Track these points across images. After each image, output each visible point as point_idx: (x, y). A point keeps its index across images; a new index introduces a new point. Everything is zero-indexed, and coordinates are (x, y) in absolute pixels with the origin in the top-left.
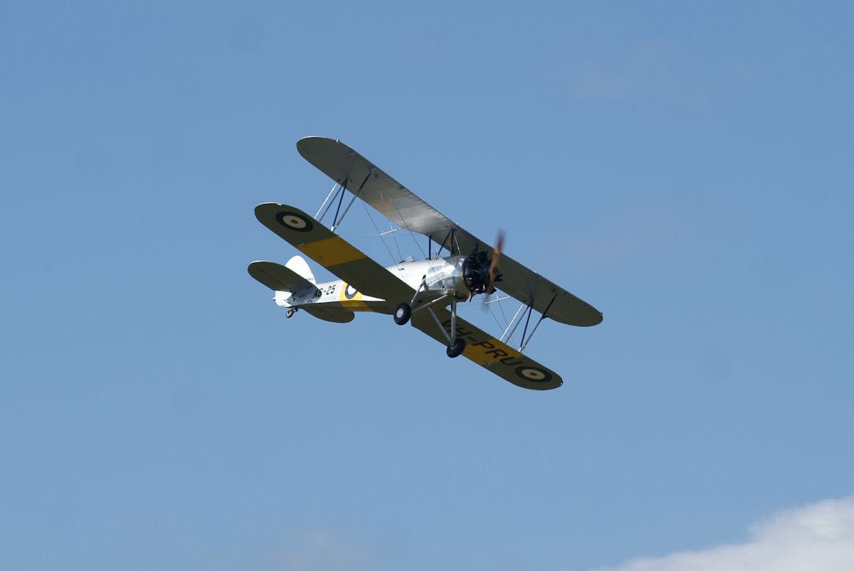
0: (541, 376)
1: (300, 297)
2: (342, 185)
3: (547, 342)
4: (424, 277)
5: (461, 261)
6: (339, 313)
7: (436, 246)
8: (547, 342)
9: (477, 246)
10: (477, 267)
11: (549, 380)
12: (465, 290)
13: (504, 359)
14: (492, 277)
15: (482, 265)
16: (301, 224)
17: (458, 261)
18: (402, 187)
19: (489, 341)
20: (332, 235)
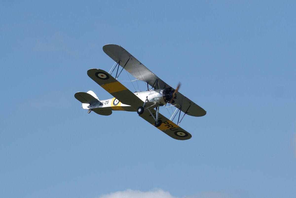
0: (184, 134)
1: (93, 106)
2: (118, 63)
3: (186, 122)
4: (147, 97)
5: (161, 91)
6: (107, 111)
7: (150, 87)
8: (186, 122)
9: (165, 86)
10: (168, 93)
11: (187, 136)
12: (163, 102)
13: (172, 127)
14: (174, 96)
15: (170, 92)
16: (105, 76)
17: (160, 91)
18: (141, 64)
19: (167, 121)
20: (117, 81)
